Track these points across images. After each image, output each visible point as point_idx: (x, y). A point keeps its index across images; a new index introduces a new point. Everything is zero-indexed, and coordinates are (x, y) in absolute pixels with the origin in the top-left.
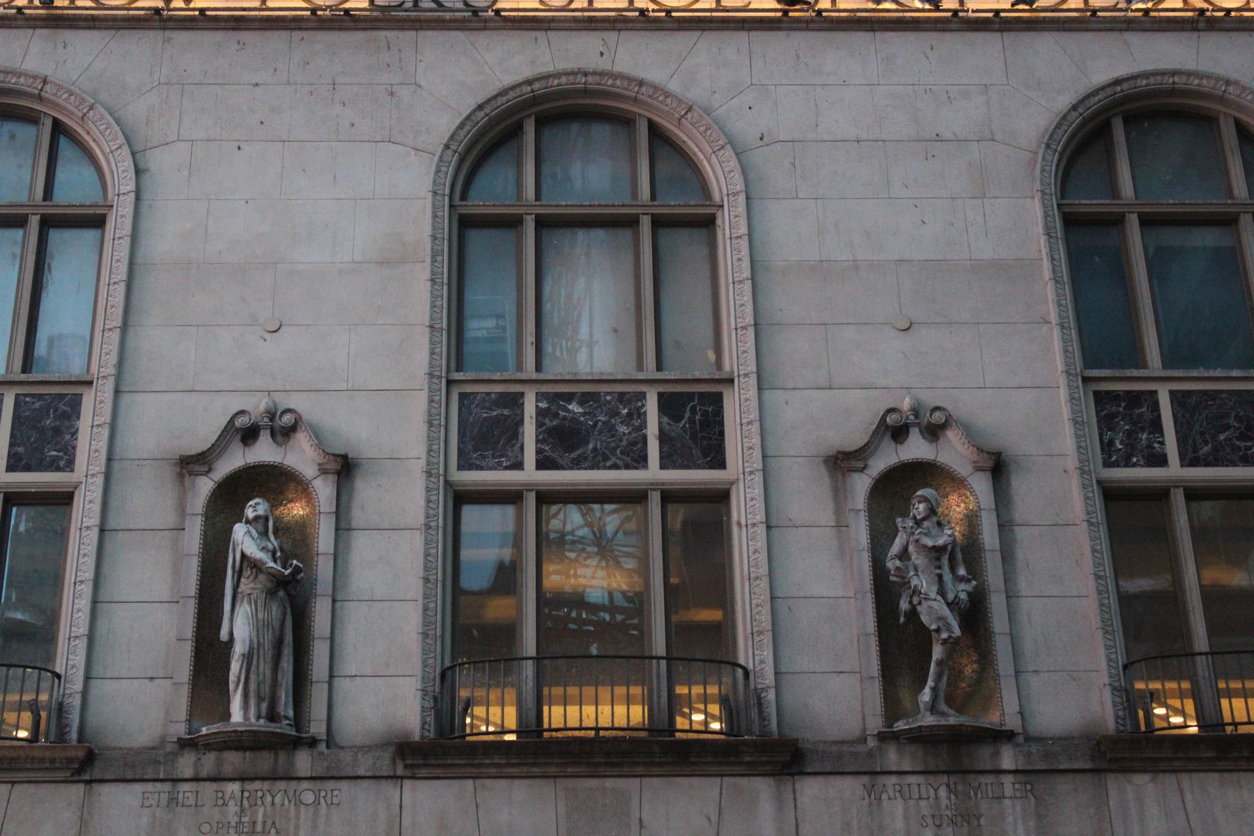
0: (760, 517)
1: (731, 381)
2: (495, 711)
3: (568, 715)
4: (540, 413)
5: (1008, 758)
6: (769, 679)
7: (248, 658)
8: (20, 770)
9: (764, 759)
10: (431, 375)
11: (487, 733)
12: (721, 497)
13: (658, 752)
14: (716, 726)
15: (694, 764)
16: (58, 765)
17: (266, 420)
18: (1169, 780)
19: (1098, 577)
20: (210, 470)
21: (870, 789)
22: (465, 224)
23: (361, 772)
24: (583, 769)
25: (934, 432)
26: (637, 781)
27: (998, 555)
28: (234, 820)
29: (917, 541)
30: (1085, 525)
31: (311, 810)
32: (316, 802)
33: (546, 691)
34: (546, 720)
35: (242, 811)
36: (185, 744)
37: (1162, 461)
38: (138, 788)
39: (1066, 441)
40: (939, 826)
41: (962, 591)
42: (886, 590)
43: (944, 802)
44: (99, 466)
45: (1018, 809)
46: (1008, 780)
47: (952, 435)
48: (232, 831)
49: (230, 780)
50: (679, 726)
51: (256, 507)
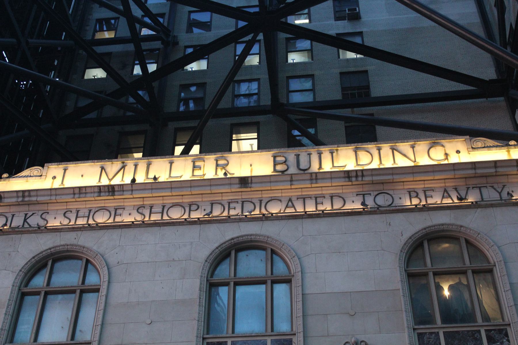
10: (197, 337)
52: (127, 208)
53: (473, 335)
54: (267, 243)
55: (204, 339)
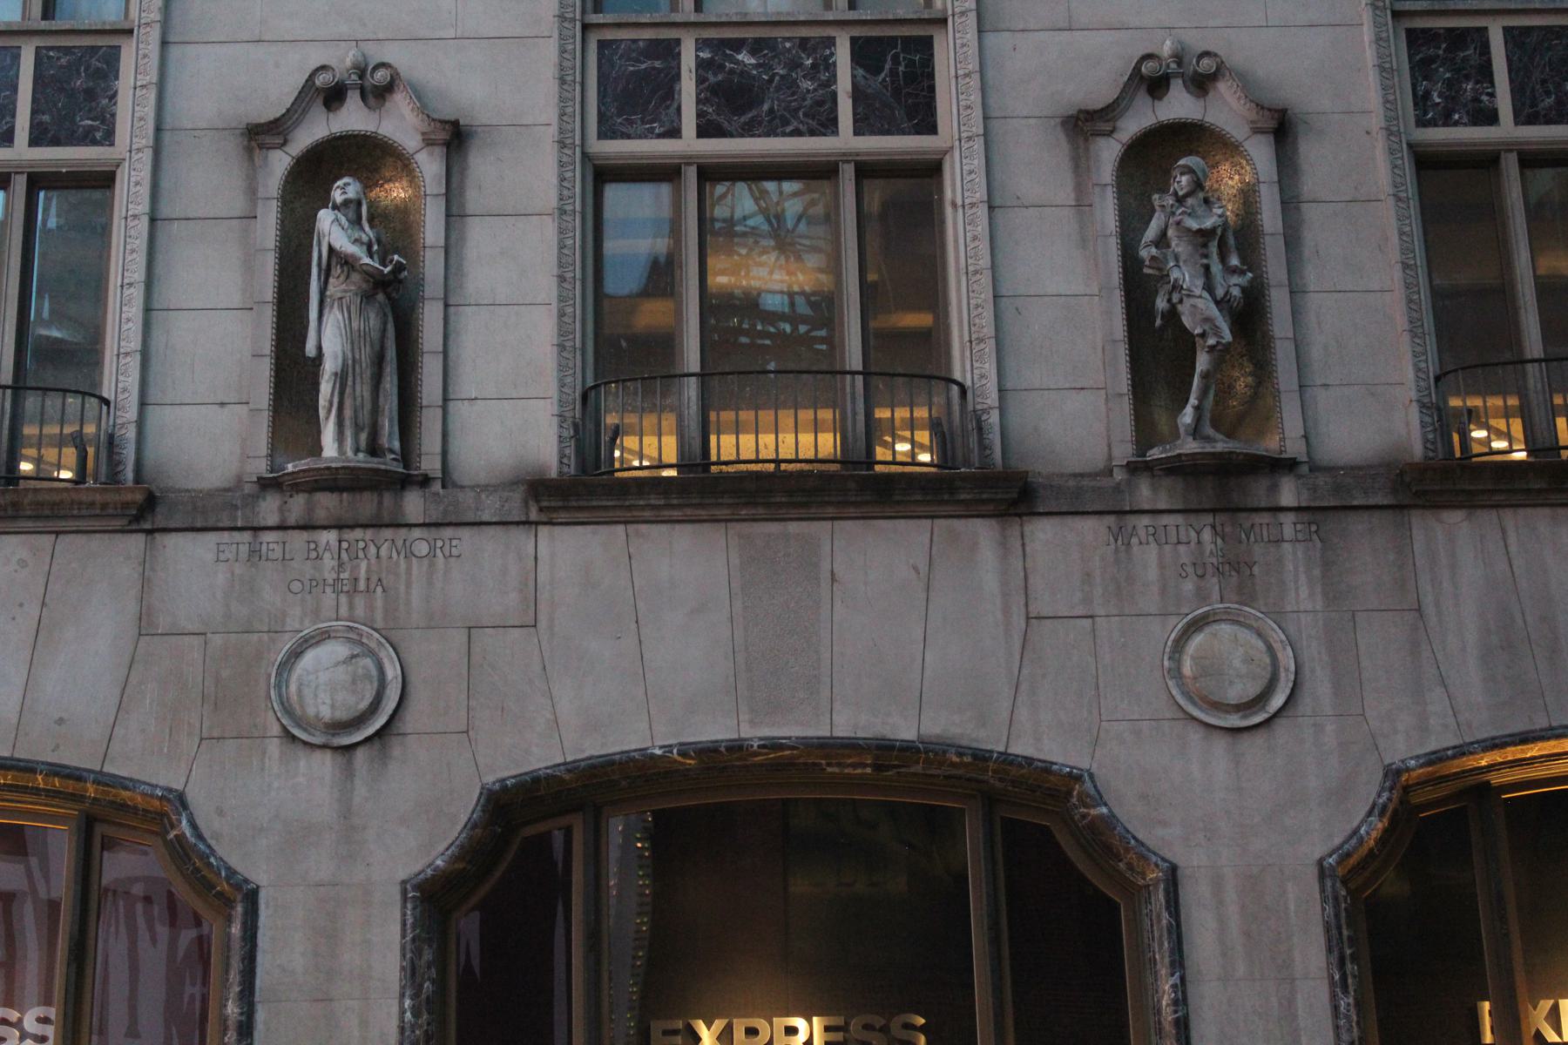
0: (981, 194)
1: (945, 21)
2: (650, 442)
4: (701, 65)
5: (1288, 493)
6: (993, 398)
7: (342, 378)
8: (65, 517)
9: (985, 496)
11: (641, 468)
12: (930, 170)
13: (854, 488)
14: (925, 457)
15: (898, 503)
16: (111, 511)
17: (354, 77)
18: (1488, 518)
19: (1405, 266)
20: (285, 143)
23: (486, 517)
24: (761, 511)
25: (1201, 84)
26: (828, 524)
28: (330, 577)
29: (1178, 223)
30: (1391, 201)
31: (426, 561)
32: (432, 554)
33: (713, 416)
34: (713, 452)
35: (340, 565)
36: (267, 485)
37: (1491, 118)
38: (212, 538)
39: (1369, 93)
40: (1202, 577)
41: (1234, 286)
42: (1138, 286)
43: (1209, 547)
45: (1300, 554)
46: (1288, 519)
47: (1224, 87)
48: (329, 590)
49: (325, 528)
50: (879, 457)
51: (345, 189)
55: (586, 27)
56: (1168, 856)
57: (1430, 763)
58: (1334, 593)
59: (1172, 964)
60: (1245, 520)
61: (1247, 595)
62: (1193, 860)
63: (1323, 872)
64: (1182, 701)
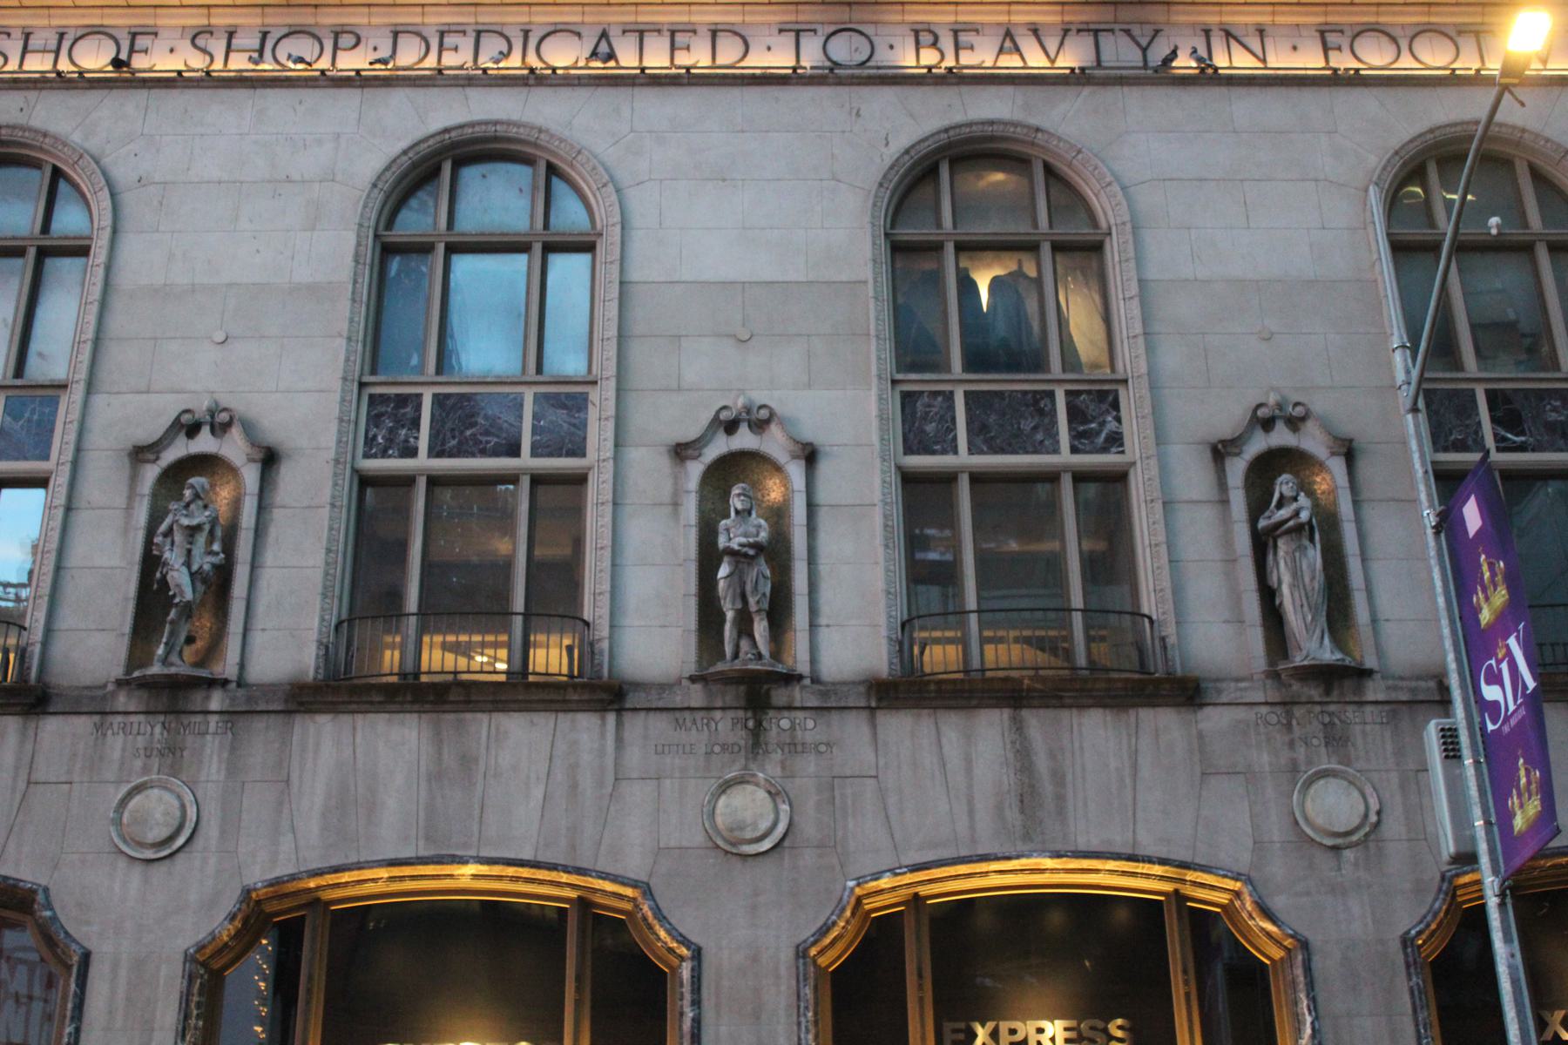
3: (437, 658)
5: (216, 701)
6: (38, 635)
10: (345, 379)
12: (579, 480)
19: (329, 551)
20: (158, 458)
21: (98, 727)
22: (387, 250)
27: (251, 535)
30: (328, 507)
33: (426, 639)
41: (203, 562)
42: (151, 562)
44: (69, 455)
46: (213, 719)
52: (163, 34)
53: (1036, 402)
54: (536, 145)
55: (362, 385)
56: (86, 944)
57: (271, 885)
58: (233, 768)
59: (72, 1018)
60: (185, 719)
61: (174, 773)
62: (103, 950)
63: (189, 958)
64: (116, 840)
